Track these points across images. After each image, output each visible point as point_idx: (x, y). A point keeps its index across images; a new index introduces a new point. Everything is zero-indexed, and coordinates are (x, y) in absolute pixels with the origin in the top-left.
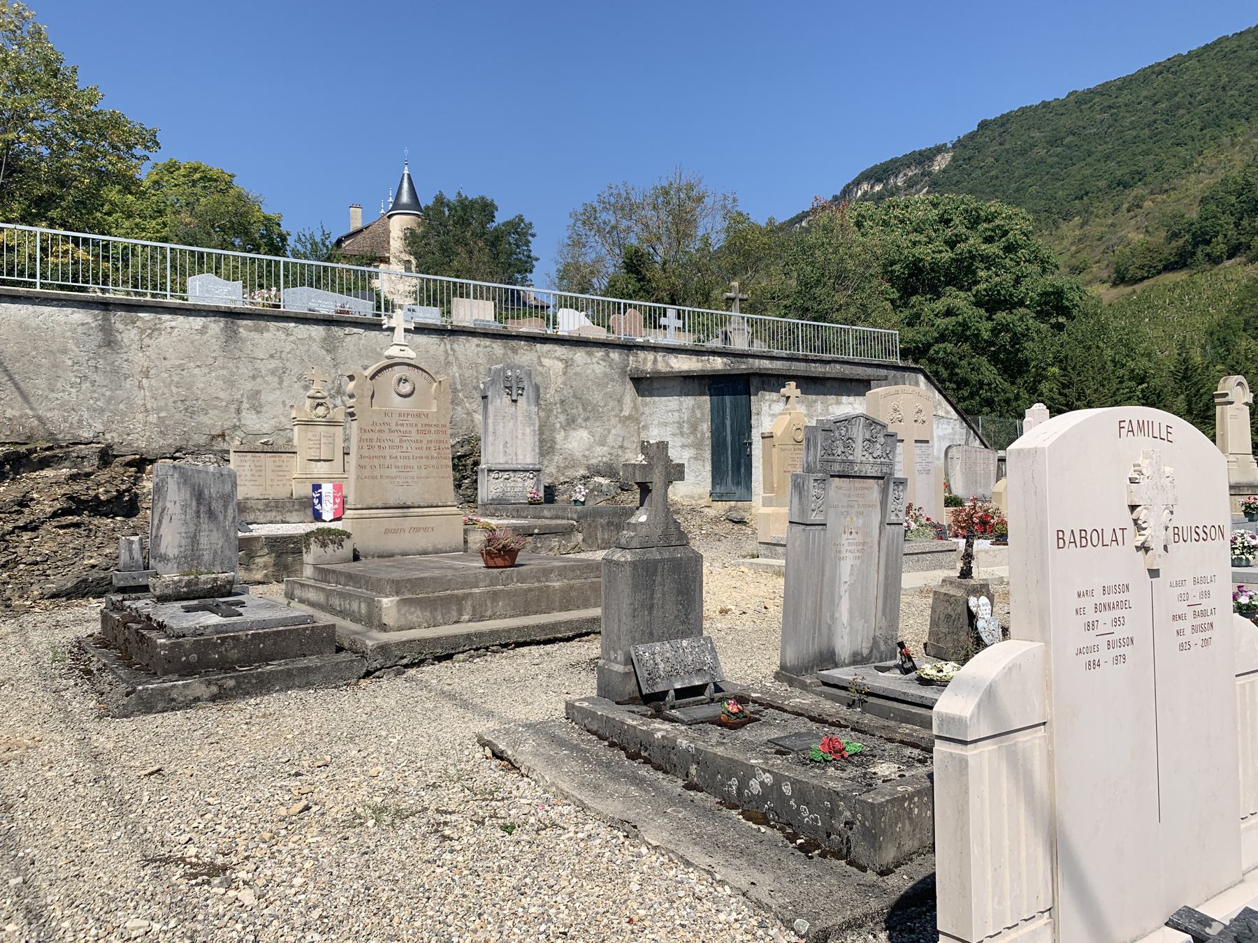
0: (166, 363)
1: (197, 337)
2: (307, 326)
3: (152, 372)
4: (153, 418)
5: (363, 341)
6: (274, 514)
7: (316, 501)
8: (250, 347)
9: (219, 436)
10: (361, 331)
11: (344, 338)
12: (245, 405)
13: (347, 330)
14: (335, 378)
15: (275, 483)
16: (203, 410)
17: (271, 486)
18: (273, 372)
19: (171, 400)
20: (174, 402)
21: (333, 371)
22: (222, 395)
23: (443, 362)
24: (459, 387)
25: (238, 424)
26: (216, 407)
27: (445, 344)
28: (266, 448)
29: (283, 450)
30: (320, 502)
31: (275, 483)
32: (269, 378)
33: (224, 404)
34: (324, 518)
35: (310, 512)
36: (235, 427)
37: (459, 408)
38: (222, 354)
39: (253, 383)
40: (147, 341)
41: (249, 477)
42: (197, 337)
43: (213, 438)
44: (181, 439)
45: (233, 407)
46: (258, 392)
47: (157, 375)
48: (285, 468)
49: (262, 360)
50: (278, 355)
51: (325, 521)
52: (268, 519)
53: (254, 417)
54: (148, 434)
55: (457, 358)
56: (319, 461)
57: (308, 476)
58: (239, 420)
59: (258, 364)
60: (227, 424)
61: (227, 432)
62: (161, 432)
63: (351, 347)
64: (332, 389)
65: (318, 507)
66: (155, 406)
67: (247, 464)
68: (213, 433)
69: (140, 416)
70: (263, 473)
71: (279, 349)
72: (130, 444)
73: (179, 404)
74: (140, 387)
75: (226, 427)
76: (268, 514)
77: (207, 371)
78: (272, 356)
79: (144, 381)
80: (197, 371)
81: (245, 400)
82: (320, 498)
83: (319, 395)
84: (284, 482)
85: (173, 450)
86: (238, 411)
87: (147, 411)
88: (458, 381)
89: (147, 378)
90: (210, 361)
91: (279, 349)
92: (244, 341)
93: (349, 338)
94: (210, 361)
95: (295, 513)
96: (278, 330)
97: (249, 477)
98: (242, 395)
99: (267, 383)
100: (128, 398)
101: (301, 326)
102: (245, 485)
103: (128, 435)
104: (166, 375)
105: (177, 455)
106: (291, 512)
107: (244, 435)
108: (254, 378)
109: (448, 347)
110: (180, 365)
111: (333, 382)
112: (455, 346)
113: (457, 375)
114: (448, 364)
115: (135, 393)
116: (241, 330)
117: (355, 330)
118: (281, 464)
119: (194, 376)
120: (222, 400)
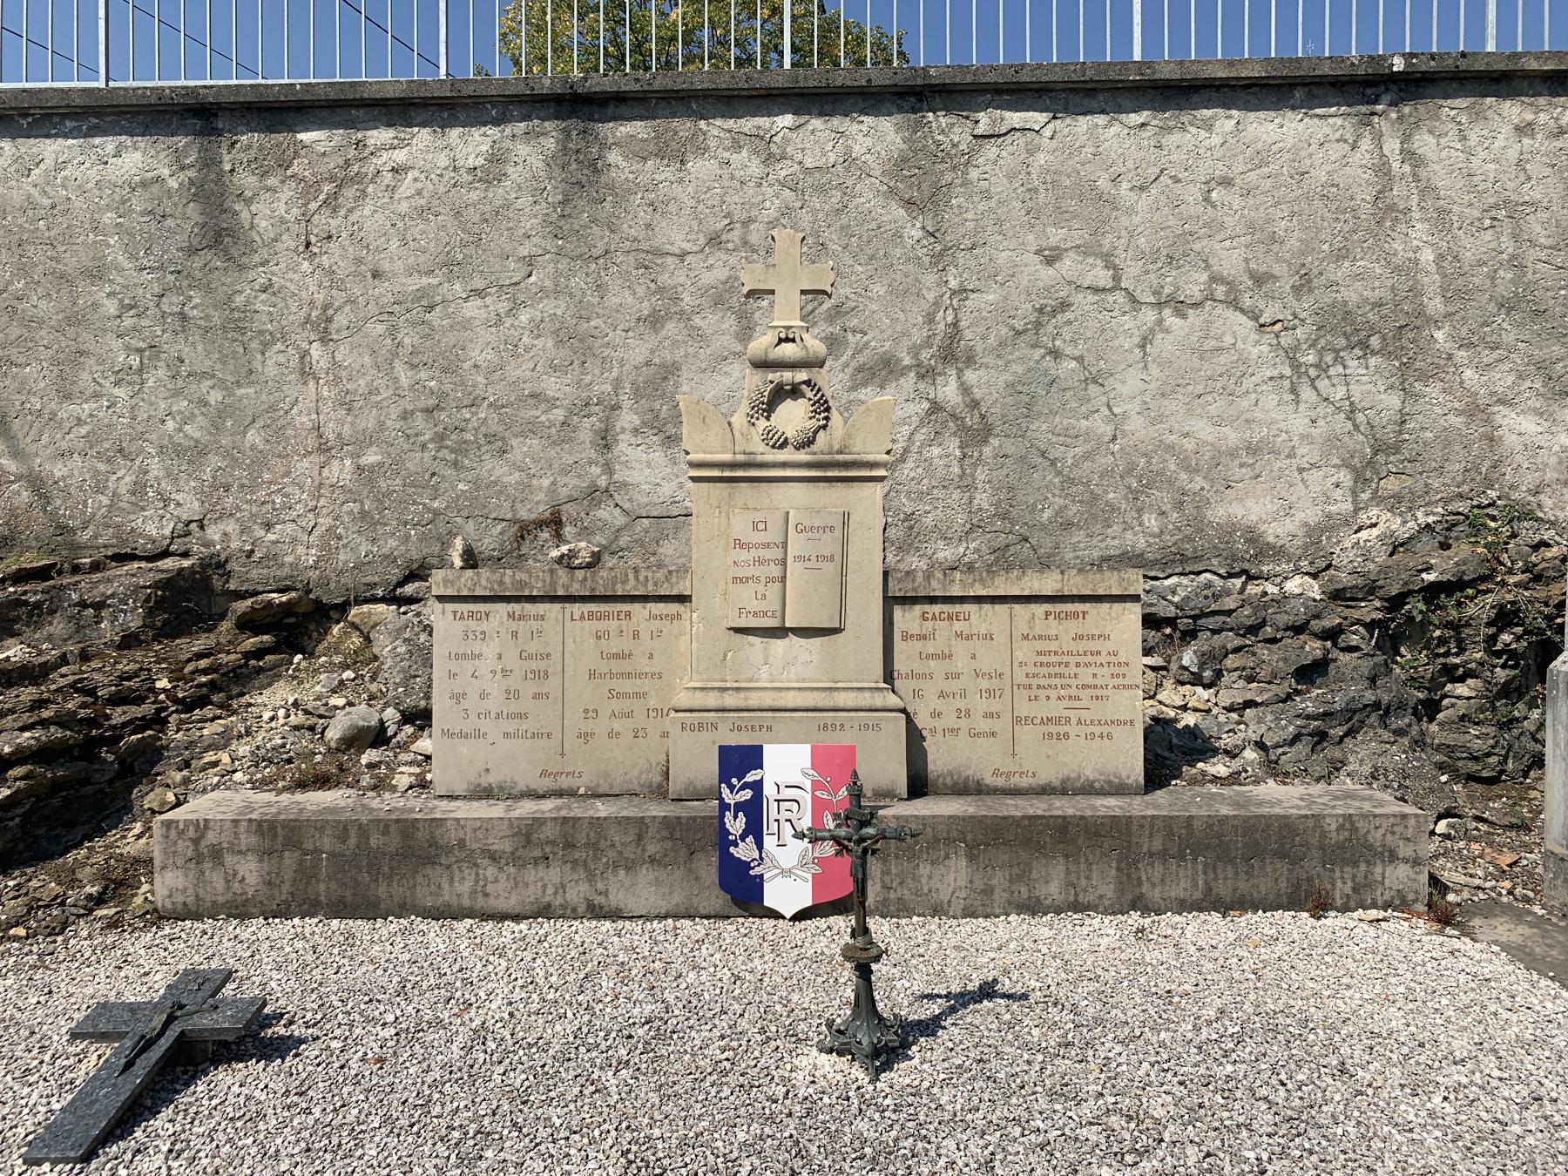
0: (381, 289)
1: (474, 196)
2: (836, 121)
3: (341, 319)
4: (341, 471)
5: (1041, 158)
6: (554, 874)
7: (736, 825)
8: (644, 216)
9: (540, 524)
10: (1036, 118)
11: (970, 154)
12: (628, 418)
13: (984, 120)
14: (937, 303)
15: (601, 726)
16: (491, 438)
17: (586, 736)
18: (718, 300)
19: (395, 411)
20: (405, 416)
21: (930, 278)
22: (552, 385)
23: (1366, 210)
24: (1435, 306)
25: (602, 482)
26: (532, 428)
27: (1378, 138)
28: (564, 582)
29: (631, 588)
30: (755, 829)
31: (601, 726)
32: (708, 321)
33: (558, 415)
34: (769, 901)
35: (708, 868)
36: (594, 495)
37: (1434, 391)
38: (549, 244)
39: (652, 340)
40: (323, 221)
41: (495, 703)
42: (474, 196)
43: (524, 531)
44: (423, 538)
45: (587, 428)
46: (670, 371)
47: (353, 329)
48: (640, 663)
49: (682, 256)
50: (735, 235)
51: (777, 915)
52: (531, 895)
53: (658, 456)
54: (325, 522)
55: (1427, 190)
56: (780, 632)
57: (730, 700)
58: (608, 469)
59: (673, 275)
60: (570, 485)
61: (569, 511)
62: (364, 515)
63: (999, 185)
64: (927, 343)
65: (744, 851)
66: (347, 431)
67: (489, 650)
68: (524, 514)
69: (304, 466)
70: (552, 684)
71: (738, 214)
72: (271, 558)
73: (419, 421)
74: (306, 372)
75: (564, 492)
76: (531, 874)
77: (503, 307)
78: (715, 241)
79: (316, 351)
80: (472, 309)
81: (626, 401)
82: (753, 811)
83: (789, 351)
84: (639, 720)
85: (395, 574)
86: (605, 440)
87: (323, 449)
88: (1431, 281)
89: (325, 340)
90: (514, 271)
91: (738, 214)
92: (621, 194)
93: (990, 150)
94: (514, 271)
95: (645, 875)
96: (737, 146)
97: (495, 703)
98: (617, 384)
99: (698, 335)
100: (272, 408)
101: (817, 123)
102: (479, 735)
103: (268, 526)
104: (380, 328)
105: (409, 589)
106: (630, 866)
107: (620, 520)
108: (654, 321)
109: (1392, 146)
110: (423, 292)
111: (930, 319)
112: (1424, 142)
113: (1427, 256)
114: (1388, 213)
115: (291, 392)
116: (614, 157)
117: (1015, 118)
118: (626, 644)
119: (466, 324)
120: (552, 403)
